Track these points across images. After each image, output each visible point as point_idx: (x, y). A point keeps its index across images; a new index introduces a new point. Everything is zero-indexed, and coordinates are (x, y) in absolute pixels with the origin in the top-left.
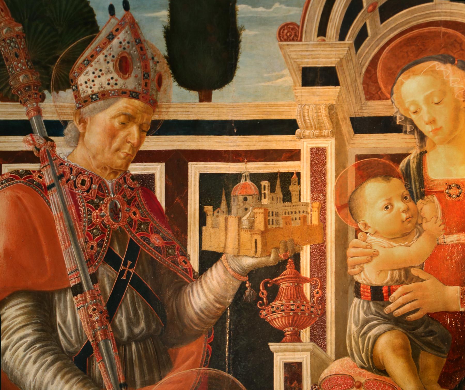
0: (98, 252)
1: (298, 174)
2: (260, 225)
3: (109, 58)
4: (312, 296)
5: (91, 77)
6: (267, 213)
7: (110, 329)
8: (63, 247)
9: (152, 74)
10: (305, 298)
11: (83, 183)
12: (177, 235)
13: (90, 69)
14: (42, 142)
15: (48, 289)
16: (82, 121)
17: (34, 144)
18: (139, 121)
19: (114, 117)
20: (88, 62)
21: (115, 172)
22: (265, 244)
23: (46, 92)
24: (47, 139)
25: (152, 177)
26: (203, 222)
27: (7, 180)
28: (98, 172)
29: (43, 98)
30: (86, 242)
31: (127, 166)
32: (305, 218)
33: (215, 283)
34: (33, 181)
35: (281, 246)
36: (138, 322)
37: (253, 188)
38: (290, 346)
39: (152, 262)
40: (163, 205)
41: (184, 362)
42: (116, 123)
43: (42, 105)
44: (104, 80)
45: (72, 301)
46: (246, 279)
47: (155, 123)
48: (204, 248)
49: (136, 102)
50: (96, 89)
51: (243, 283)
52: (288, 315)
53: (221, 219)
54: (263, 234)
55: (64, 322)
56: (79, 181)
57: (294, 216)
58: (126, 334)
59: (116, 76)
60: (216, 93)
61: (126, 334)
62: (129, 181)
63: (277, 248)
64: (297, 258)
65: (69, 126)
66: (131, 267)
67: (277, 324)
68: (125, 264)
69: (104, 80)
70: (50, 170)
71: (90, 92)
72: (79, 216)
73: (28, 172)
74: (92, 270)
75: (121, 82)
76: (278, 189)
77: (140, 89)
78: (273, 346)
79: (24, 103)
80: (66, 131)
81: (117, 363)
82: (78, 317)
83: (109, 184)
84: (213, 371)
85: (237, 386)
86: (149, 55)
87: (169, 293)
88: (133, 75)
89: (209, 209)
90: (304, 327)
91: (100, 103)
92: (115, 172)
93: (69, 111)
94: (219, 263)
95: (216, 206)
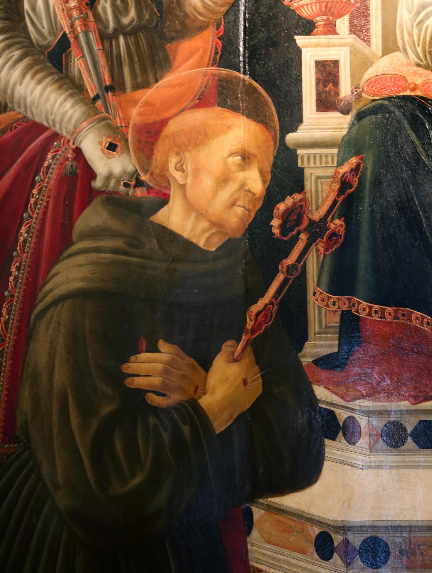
7: (91, 18)
36: (126, 11)
38: (323, 39)
41: (186, 60)
55: (34, 9)
58: (112, 25)
61: (112, 25)
67: (306, 13)
78: (300, 40)
81: (102, 61)
84: (224, 72)
85: (255, 89)
90: (340, 16)
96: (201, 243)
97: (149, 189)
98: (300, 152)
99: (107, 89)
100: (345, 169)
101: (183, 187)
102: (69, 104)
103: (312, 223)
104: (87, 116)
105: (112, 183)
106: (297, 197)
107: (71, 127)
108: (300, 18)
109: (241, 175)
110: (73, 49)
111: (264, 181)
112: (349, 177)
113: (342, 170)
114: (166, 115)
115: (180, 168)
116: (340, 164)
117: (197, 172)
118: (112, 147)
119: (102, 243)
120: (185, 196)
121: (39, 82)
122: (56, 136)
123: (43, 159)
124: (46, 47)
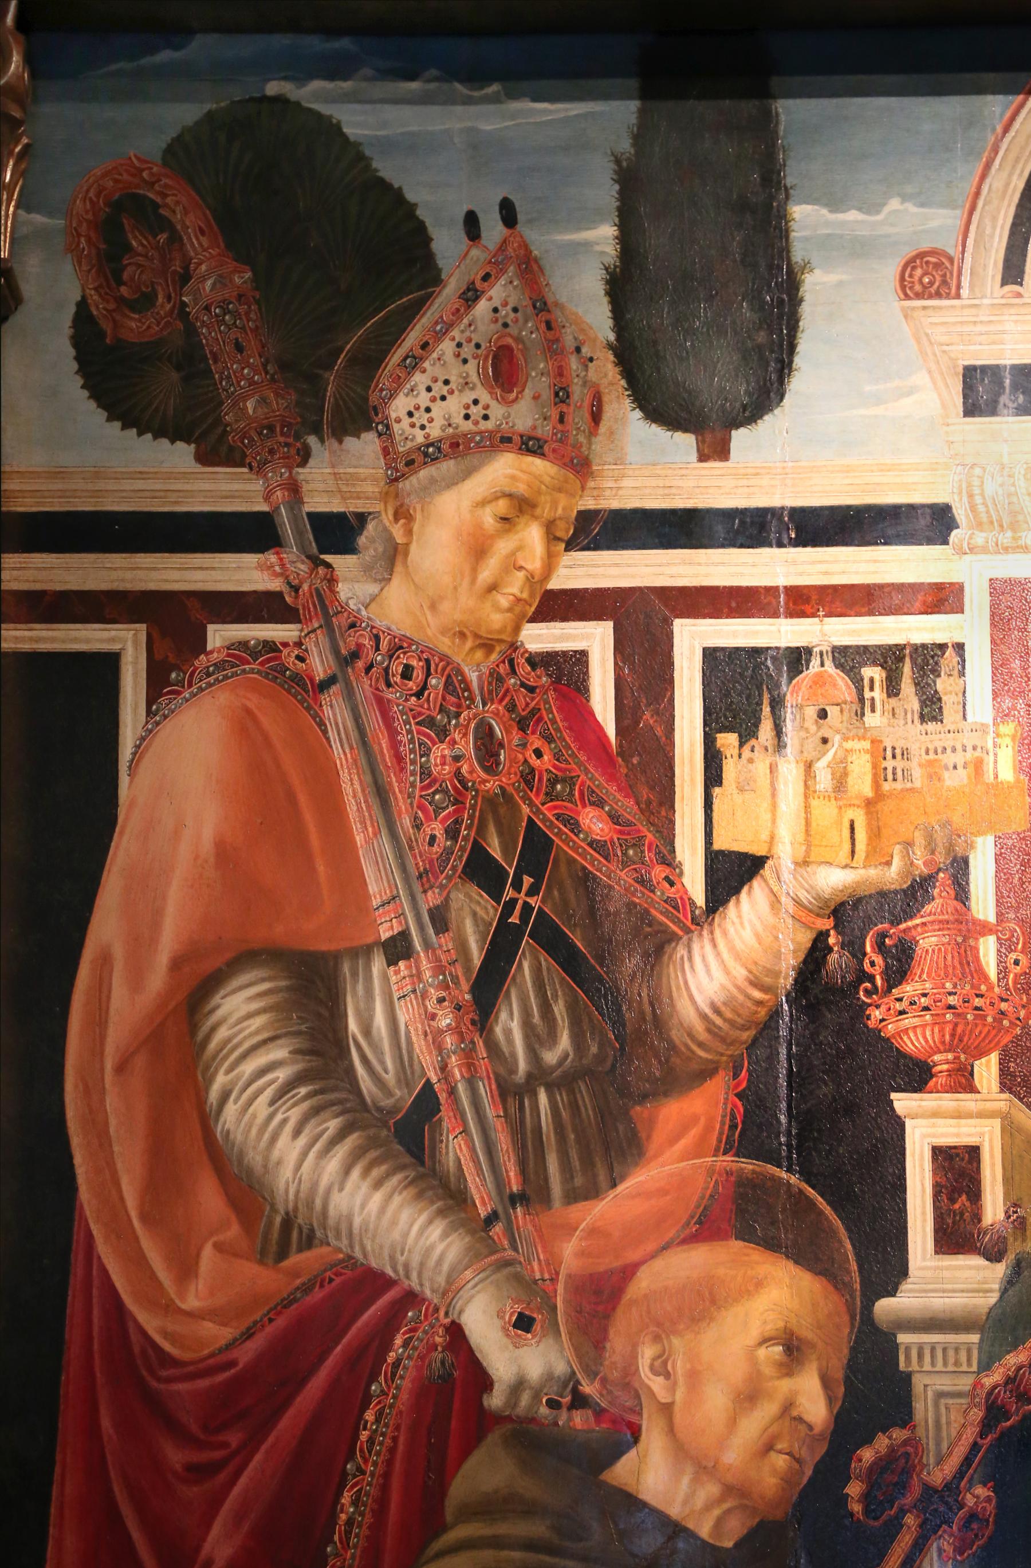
0: (448, 852)
1: (960, 647)
2: (861, 783)
3: (467, 351)
4: (1003, 972)
5: (424, 399)
6: (879, 752)
7: (482, 1051)
8: (359, 839)
9: (577, 391)
10: (986, 978)
11: (407, 673)
12: (647, 810)
13: (419, 379)
14: (303, 567)
15: (323, 947)
16: (403, 514)
17: (284, 575)
18: (545, 511)
19: (483, 503)
20: (413, 363)
21: (488, 646)
22: (875, 834)
23: (312, 440)
24: (316, 562)
25: (581, 658)
26: (713, 776)
27: (220, 666)
28: (445, 645)
29: (305, 456)
30: (418, 826)
31: (517, 629)
32: (978, 766)
33: (748, 934)
34: (283, 669)
35: (919, 839)
36: (552, 1037)
37: (842, 685)
38: (947, 1101)
39: (585, 880)
40: (611, 730)
41: (673, 1141)
42: (488, 519)
43: (302, 473)
44: (454, 406)
45: (385, 978)
46: (827, 924)
47: (586, 518)
48: (720, 843)
49: (538, 465)
50: (435, 431)
51: (821, 937)
52: (938, 1021)
53: (761, 766)
54: (869, 804)
55: (367, 1031)
56: (397, 668)
57: (949, 758)
58: (522, 1065)
59: (484, 397)
60: (739, 437)
61: (522, 1065)
62: (523, 668)
63: (909, 844)
64: (960, 867)
65: (371, 526)
66: (533, 891)
67: (913, 1044)
68: (517, 885)
69: (454, 406)
70: (322, 637)
71: (420, 438)
72: (399, 758)
73: (270, 647)
74: (433, 898)
75: (497, 411)
76: (907, 687)
77: (545, 430)
78: (902, 1102)
79: (258, 469)
80: (362, 540)
81: (503, 1141)
82: (402, 1018)
83: (473, 677)
84: (748, 1166)
85: (812, 1204)
86: (569, 342)
87: (631, 963)
88: (528, 393)
89: (728, 741)
90: (982, 1053)
91: (448, 466)
92: (488, 646)
93: (370, 488)
94: (756, 883)
95: (747, 733)
96: (705, 1531)
97: (600, 1413)
98: (903, 1338)
99: (514, 1200)
100: (994, 1378)
101: (667, 1409)
102: (436, 1231)
103: (929, 1490)
104: (473, 1256)
105: (525, 1399)
106: (899, 1434)
107: (441, 1280)
108: (901, 1054)
109: (785, 1385)
110: (446, 1116)
111: (830, 1400)
112: (1004, 1396)
113: (988, 1381)
114: (633, 1256)
116: (985, 1366)
117: (694, 1377)
118: (524, 1323)
119: (502, 1529)
120: (671, 1430)
121: (378, 1185)
122: (412, 1298)
123: (387, 1346)
124: (392, 1111)
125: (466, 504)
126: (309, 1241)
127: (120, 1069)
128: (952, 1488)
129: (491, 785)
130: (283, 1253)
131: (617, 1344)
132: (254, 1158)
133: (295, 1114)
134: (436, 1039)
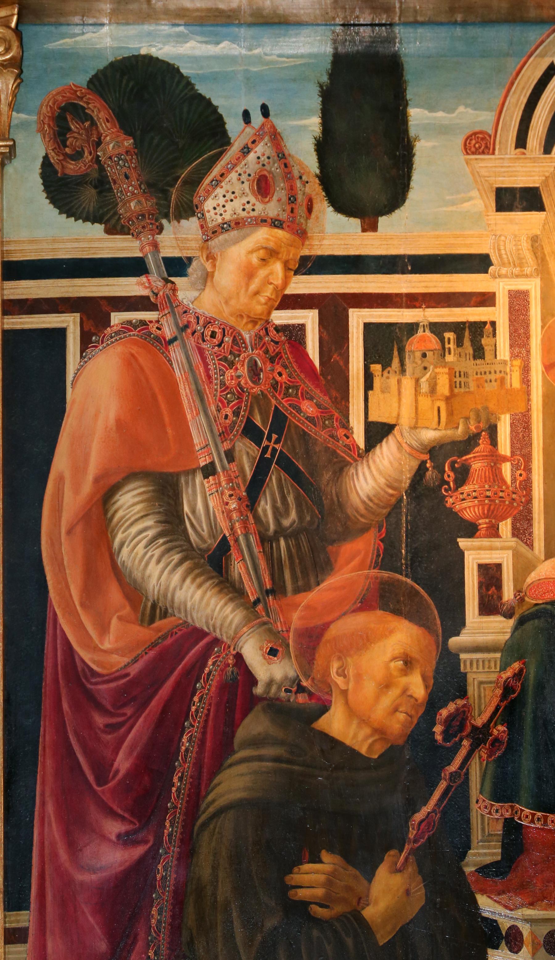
11: (213, 335)
14: (160, 284)
28: (232, 321)
30: (219, 410)
36: (287, 513)
55: (194, 511)
56: (208, 333)
58: (272, 527)
61: (272, 527)
65: (194, 264)
70: (171, 319)
73: (143, 323)
74: (227, 445)
81: (262, 564)
92: (254, 322)
96: (363, 751)
97: (311, 695)
99: (268, 592)
101: (345, 693)
102: (229, 609)
103: (475, 728)
104: (247, 621)
105: (274, 689)
106: (460, 702)
109: (404, 680)
110: (233, 552)
111: (426, 687)
115: (342, 673)
117: (359, 677)
118: (273, 652)
120: (347, 703)
122: (216, 641)
125: (243, 252)
126: (165, 614)
127: (69, 532)
128: (487, 726)
129: (256, 390)
130: (152, 620)
131: (319, 661)
132: (137, 574)
133: (157, 552)
134: (228, 515)
